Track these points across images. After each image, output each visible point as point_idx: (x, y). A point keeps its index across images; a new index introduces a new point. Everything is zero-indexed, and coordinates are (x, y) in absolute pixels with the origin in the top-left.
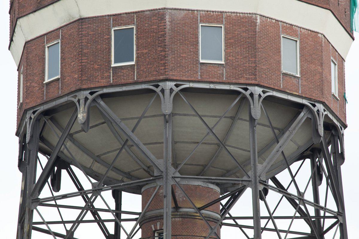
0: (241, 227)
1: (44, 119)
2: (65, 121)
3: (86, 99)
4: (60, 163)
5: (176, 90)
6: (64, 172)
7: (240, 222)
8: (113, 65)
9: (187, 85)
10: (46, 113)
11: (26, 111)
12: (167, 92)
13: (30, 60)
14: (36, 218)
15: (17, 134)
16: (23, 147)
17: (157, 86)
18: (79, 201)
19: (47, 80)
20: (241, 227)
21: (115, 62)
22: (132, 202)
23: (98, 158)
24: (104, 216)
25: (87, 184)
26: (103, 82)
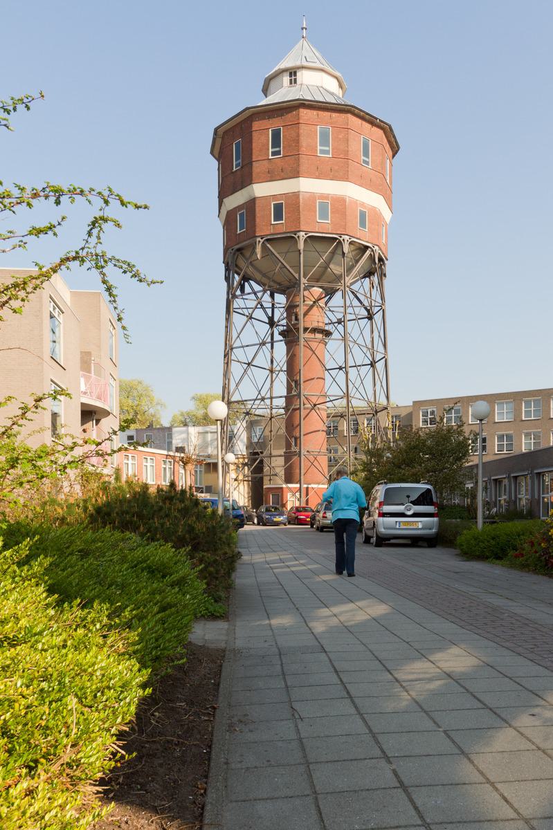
0: (332, 311)
1: (237, 253)
2: (248, 254)
3: (259, 242)
4: (246, 279)
5: (306, 236)
6: (246, 284)
7: (331, 309)
8: (273, 223)
9: (310, 234)
10: (239, 250)
11: (228, 249)
12: (301, 238)
13: (229, 223)
14: (235, 305)
15: (223, 263)
16: (226, 270)
17: (295, 234)
18: (253, 296)
19: (239, 232)
20: (332, 311)
21: (274, 221)
22: (281, 299)
23: (264, 275)
24: (265, 305)
25: (257, 288)
26: (268, 233)
